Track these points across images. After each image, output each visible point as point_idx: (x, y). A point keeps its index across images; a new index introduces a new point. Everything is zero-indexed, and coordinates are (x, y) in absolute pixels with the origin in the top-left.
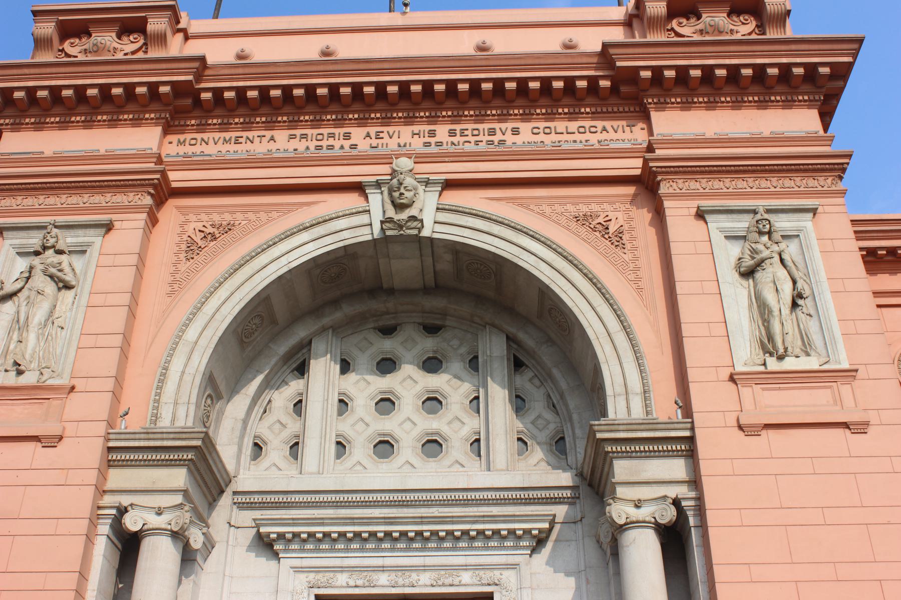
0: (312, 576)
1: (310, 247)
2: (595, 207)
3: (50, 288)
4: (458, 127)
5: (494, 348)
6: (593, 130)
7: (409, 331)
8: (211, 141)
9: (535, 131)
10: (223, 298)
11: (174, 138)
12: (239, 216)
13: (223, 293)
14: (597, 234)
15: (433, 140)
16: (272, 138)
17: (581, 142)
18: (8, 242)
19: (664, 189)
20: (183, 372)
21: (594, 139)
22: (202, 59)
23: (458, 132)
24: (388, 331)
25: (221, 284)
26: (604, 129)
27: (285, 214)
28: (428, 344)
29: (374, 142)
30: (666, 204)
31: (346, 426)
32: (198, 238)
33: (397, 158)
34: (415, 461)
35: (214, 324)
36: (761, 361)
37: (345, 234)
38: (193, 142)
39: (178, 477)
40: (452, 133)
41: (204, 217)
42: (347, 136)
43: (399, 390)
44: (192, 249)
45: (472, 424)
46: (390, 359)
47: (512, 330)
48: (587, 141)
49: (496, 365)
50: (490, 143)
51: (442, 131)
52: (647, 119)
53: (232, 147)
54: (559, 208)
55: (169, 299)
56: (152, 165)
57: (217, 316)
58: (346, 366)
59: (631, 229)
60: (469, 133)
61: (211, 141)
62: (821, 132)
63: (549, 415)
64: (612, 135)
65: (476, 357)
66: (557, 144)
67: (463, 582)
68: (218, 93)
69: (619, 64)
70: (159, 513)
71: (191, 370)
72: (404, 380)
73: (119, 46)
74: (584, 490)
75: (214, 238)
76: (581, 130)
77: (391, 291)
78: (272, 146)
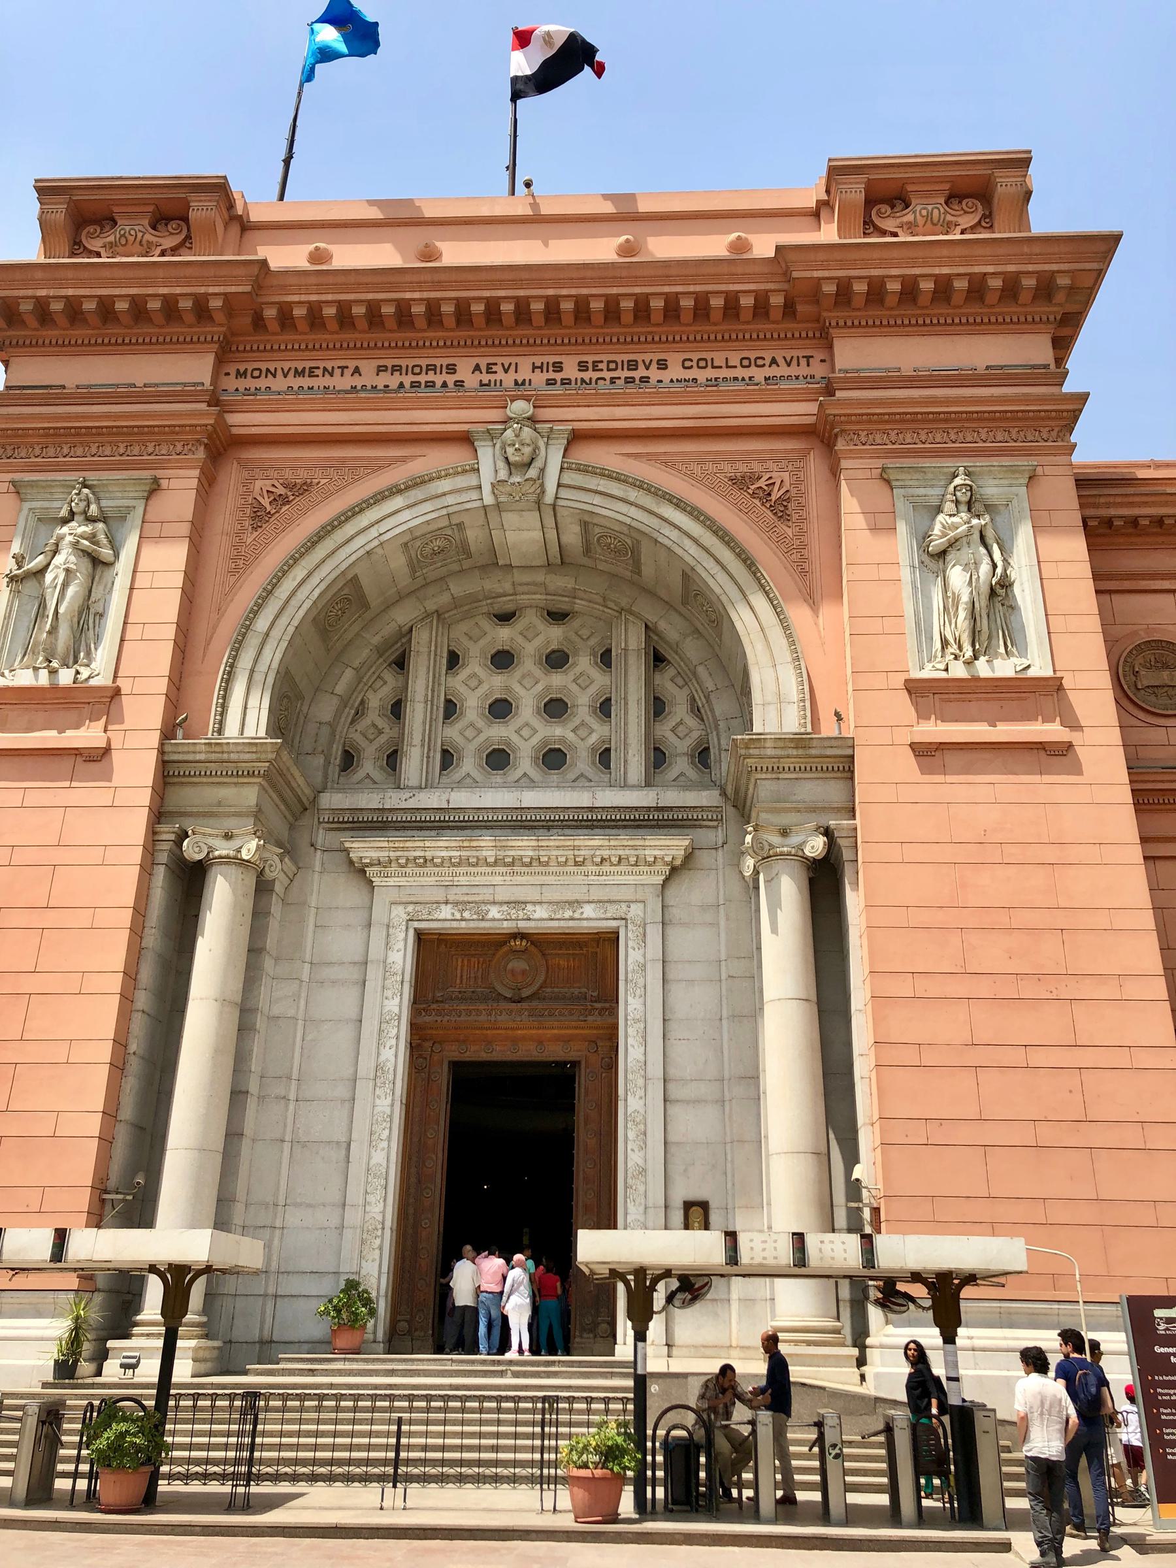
0: (410, 908)
1: (406, 515)
2: (757, 467)
3: (86, 564)
4: (590, 359)
6: (760, 362)
7: (531, 618)
8: (279, 372)
9: (687, 364)
10: (299, 579)
11: (232, 369)
12: (318, 473)
13: (299, 573)
14: (757, 502)
15: (558, 376)
16: (357, 371)
17: (743, 379)
18: (27, 505)
19: (840, 445)
20: (252, 671)
21: (759, 374)
22: (264, 263)
23: (590, 366)
24: (505, 618)
25: (296, 561)
26: (774, 361)
27: (375, 471)
28: (554, 635)
29: (486, 378)
30: (844, 464)
31: (453, 732)
33: (512, 401)
34: (534, 773)
35: (290, 610)
36: (942, 666)
37: (450, 500)
38: (256, 373)
39: (249, 795)
40: (583, 367)
41: (272, 473)
42: (452, 369)
43: (517, 688)
44: (259, 517)
45: (598, 732)
46: (508, 652)
47: (652, 618)
48: (750, 378)
49: (632, 660)
50: (629, 380)
52: (830, 347)
53: (306, 382)
54: (710, 467)
55: (233, 579)
56: (203, 406)
57: (294, 602)
58: (454, 660)
59: (801, 494)
60: (600, 366)
61: (279, 372)
62: (1053, 366)
63: (691, 722)
64: (782, 370)
65: (609, 651)
66: (713, 382)
67: (585, 916)
69: (795, 274)
70: (228, 836)
71: (262, 667)
72: (523, 677)
73: (154, 239)
74: (731, 811)
76: (746, 363)
78: (358, 382)
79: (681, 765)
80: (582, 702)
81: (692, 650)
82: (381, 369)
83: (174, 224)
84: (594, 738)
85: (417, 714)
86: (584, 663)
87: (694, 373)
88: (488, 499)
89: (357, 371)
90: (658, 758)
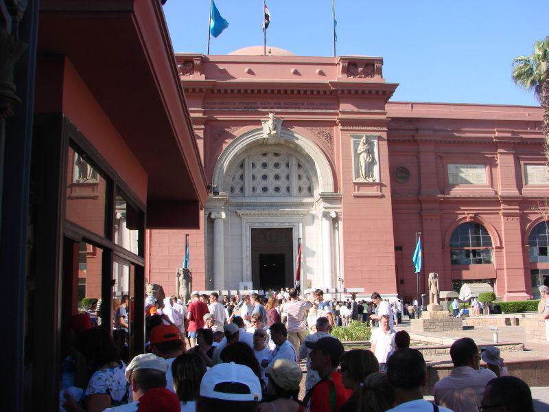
5: (294, 162)
7: (270, 156)
24: (264, 155)
26: (327, 104)
28: (276, 160)
31: (255, 183)
32: (217, 136)
40: (285, 103)
42: (256, 103)
47: (298, 158)
51: (282, 102)
58: (253, 165)
63: (307, 181)
68: (219, 91)
75: (221, 135)
77: (266, 145)
79: (305, 191)
80: (283, 176)
81: (308, 166)
82: (240, 103)
83: (189, 64)
84: (285, 185)
85: (248, 178)
86: (283, 167)
87: (310, 106)
88: (267, 136)
89: (234, 104)
90: (300, 189)
